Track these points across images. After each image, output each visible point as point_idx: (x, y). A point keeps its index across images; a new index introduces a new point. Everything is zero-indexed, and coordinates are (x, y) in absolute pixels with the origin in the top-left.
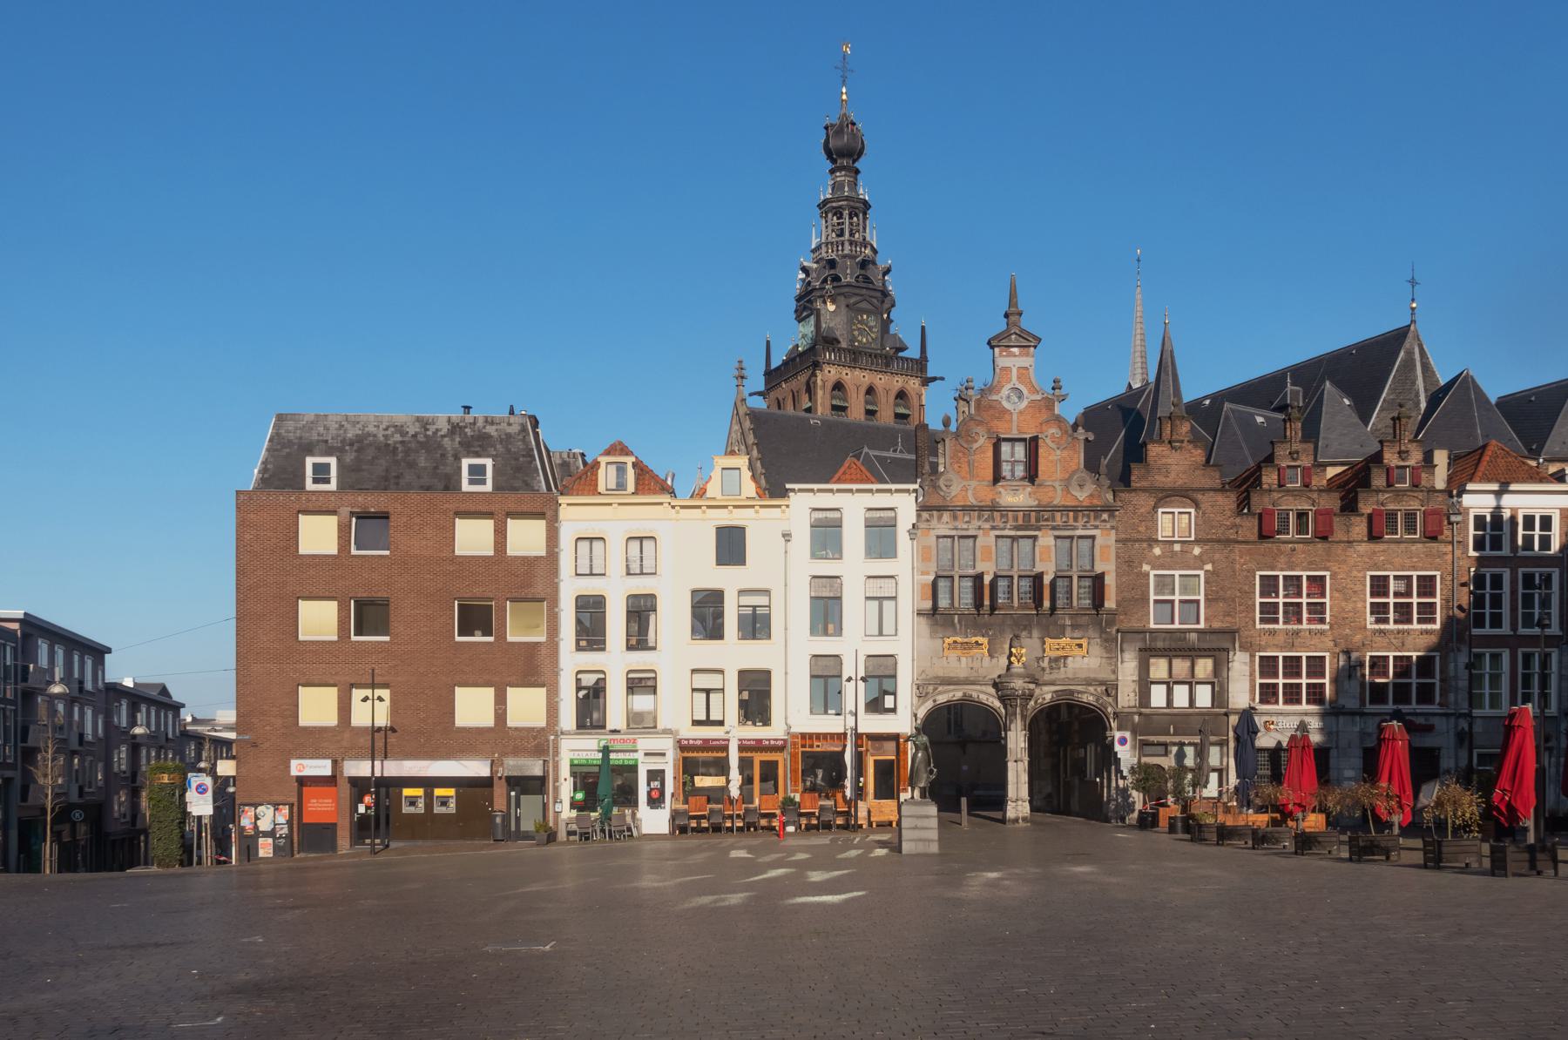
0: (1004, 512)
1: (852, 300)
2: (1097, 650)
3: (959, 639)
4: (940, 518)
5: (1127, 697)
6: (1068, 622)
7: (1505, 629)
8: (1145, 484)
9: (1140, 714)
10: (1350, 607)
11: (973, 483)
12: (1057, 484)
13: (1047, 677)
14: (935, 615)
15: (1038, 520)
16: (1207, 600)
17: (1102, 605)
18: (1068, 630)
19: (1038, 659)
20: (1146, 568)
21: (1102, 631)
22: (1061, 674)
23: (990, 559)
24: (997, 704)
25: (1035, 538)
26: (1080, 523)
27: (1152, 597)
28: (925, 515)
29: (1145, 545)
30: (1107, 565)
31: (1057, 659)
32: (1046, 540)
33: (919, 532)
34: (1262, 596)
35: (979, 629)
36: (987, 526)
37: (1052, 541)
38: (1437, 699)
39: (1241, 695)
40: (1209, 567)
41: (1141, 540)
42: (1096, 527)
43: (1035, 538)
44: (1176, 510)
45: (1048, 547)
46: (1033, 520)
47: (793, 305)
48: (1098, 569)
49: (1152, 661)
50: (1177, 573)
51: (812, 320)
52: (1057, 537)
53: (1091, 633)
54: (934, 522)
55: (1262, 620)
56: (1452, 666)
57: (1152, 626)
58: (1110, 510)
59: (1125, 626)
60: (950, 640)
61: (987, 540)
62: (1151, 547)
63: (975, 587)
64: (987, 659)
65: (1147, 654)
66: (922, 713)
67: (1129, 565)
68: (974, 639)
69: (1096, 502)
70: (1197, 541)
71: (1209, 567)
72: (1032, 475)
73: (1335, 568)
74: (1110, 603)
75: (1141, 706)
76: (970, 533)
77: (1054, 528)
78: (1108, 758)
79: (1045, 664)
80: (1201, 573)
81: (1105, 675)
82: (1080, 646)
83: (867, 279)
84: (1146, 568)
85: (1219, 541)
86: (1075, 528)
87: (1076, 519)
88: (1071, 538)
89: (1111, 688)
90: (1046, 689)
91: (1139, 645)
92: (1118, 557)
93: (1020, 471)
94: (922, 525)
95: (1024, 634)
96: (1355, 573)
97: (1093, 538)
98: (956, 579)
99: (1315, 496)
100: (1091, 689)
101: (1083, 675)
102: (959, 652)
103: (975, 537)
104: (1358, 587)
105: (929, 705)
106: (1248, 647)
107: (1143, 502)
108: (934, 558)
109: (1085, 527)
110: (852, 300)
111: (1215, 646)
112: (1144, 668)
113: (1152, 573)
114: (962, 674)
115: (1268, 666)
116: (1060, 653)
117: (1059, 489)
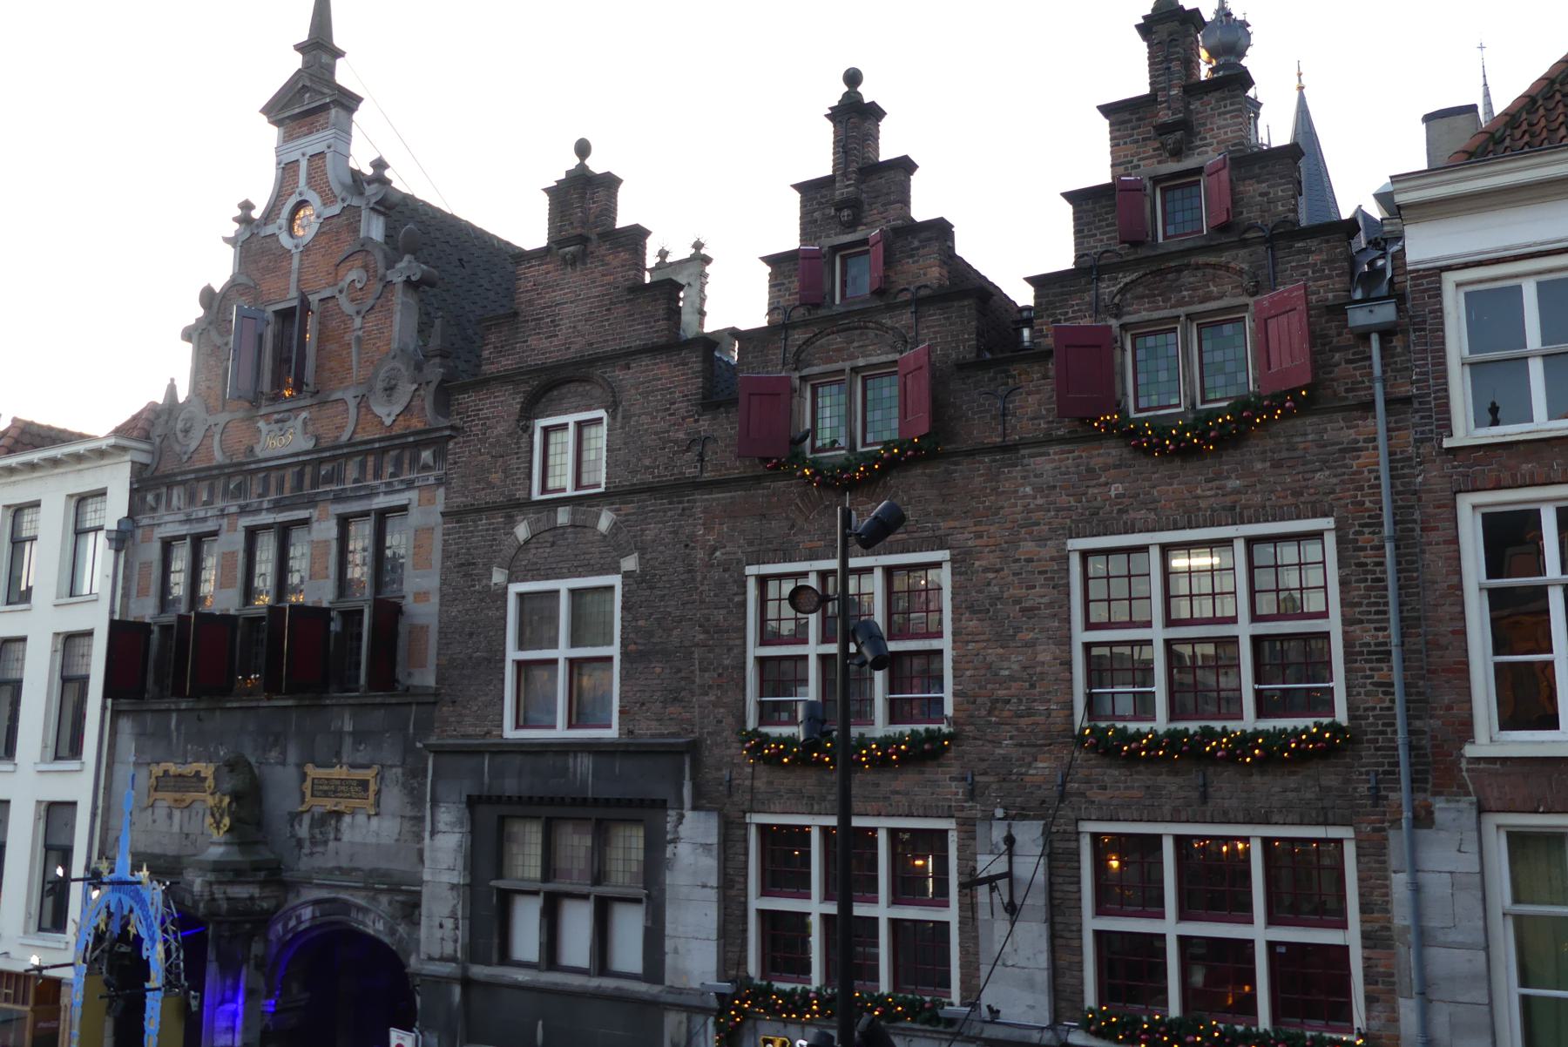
2: (394, 798)
3: (173, 769)
6: (348, 727)
8: (507, 363)
9: (467, 983)
10: (1014, 663)
22: (330, 857)
40: (630, 563)
42: (410, 485)
50: (563, 586)
56: (1399, 883)
57: (510, 732)
58: (438, 443)
60: (158, 770)
62: (511, 521)
67: (464, 571)
71: (630, 563)
73: (966, 538)
75: (474, 953)
76: (210, 526)
77: (339, 498)
79: (303, 831)
80: (615, 580)
84: (498, 577)
85: (651, 490)
86: (372, 494)
91: (468, 787)
92: (446, 556)
96: (1028, 547)
99: (905, 318)
104: (1040, 595)
107: (501, 405)
115: (784, 859)
116: (329, 804)
117: (352, 404)
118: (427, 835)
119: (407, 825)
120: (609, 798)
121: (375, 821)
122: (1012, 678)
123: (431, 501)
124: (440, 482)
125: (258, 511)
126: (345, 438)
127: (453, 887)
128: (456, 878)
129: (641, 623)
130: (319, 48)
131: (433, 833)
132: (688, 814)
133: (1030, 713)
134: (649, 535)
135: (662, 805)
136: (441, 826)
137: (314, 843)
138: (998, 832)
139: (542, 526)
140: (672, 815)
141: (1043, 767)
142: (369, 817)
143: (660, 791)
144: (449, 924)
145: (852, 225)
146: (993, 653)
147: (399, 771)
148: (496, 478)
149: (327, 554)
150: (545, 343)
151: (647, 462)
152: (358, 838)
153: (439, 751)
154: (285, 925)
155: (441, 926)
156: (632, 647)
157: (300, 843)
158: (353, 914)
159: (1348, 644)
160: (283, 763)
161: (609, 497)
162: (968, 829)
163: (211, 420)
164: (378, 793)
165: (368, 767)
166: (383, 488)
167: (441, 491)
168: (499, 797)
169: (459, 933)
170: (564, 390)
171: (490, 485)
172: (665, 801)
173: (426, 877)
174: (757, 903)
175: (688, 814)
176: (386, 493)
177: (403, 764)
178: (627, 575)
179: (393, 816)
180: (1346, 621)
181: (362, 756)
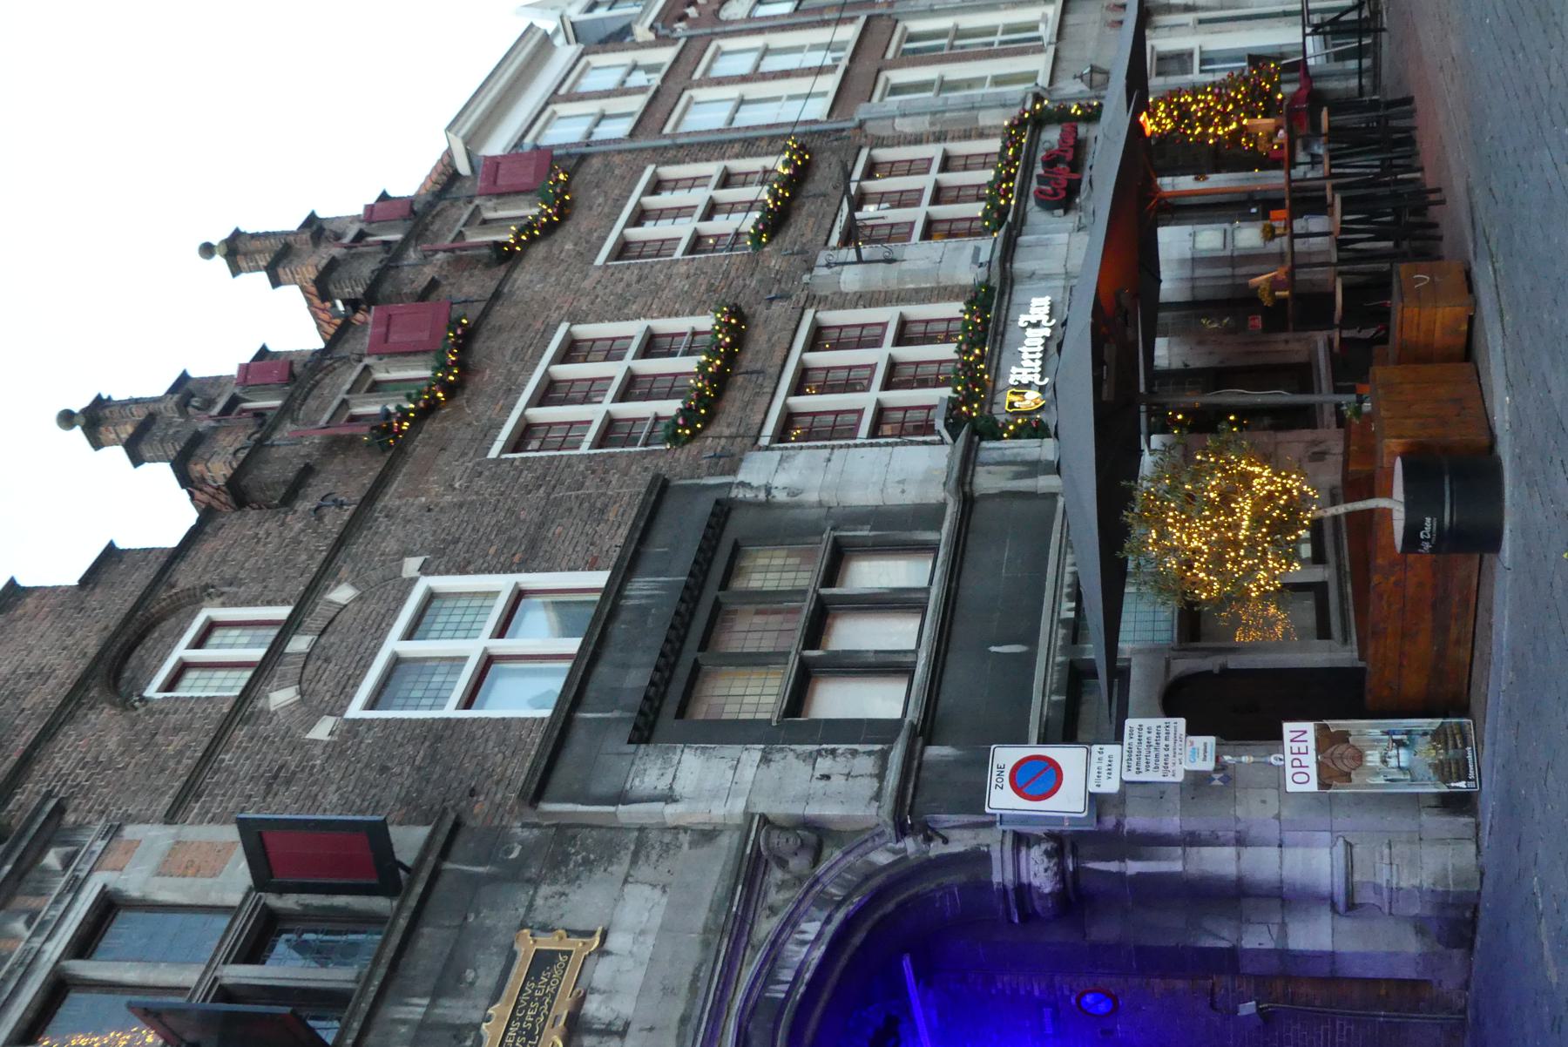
2: (586, 901)
16: (524, 566)
18: (454, 1010)
20: (322, 731)
21: (515, 874)
27: (450, 711)
29: (241, 734)
42: (76, 886)
44: (182, 651)
50: (394, 643)
81: (710, 873)
84: (322, 731)
91: (616, 742)
96: (587, 284)
97: (109, 907)
100: (766, 927)
113: (355, 710)
118: (671, 812)
119: (644, 871)
122: (693, 285)
123: (134, 844)
124: (113, 832)
127: (766, 759)
128: (754, 753)
129: (492, 551)
132: (741, 477)
133: (726, 274)
135: (724, 510)
136: (663, 785)
139: (292, 670)
142: (602, 952)
143: (704, 506)
144: (824, 764)
145: (210, 403)
146: (667, 294)
147: (545, 890)
148: (178, 741)
150: (46, 689)
151: (304, 557)
152: (635, 977)
153: (538, 790)
155: (827, 777)
156: (516, 559)
158: (779, 992)
159: (737, 156)
162: (813, 300)
164: (571, 932)
165: (511, 957)
166: (37, 942)
167: (130, 831)
168: (646, 698)
169: (842, 748)
170: (133, 661)
171: (180, 753)
172: (718, 502)
175: (741, 477)
176: (49, 938)
177: (535, 883)
178: (425, 570)
179: (618, 900)
180: (722, 157)
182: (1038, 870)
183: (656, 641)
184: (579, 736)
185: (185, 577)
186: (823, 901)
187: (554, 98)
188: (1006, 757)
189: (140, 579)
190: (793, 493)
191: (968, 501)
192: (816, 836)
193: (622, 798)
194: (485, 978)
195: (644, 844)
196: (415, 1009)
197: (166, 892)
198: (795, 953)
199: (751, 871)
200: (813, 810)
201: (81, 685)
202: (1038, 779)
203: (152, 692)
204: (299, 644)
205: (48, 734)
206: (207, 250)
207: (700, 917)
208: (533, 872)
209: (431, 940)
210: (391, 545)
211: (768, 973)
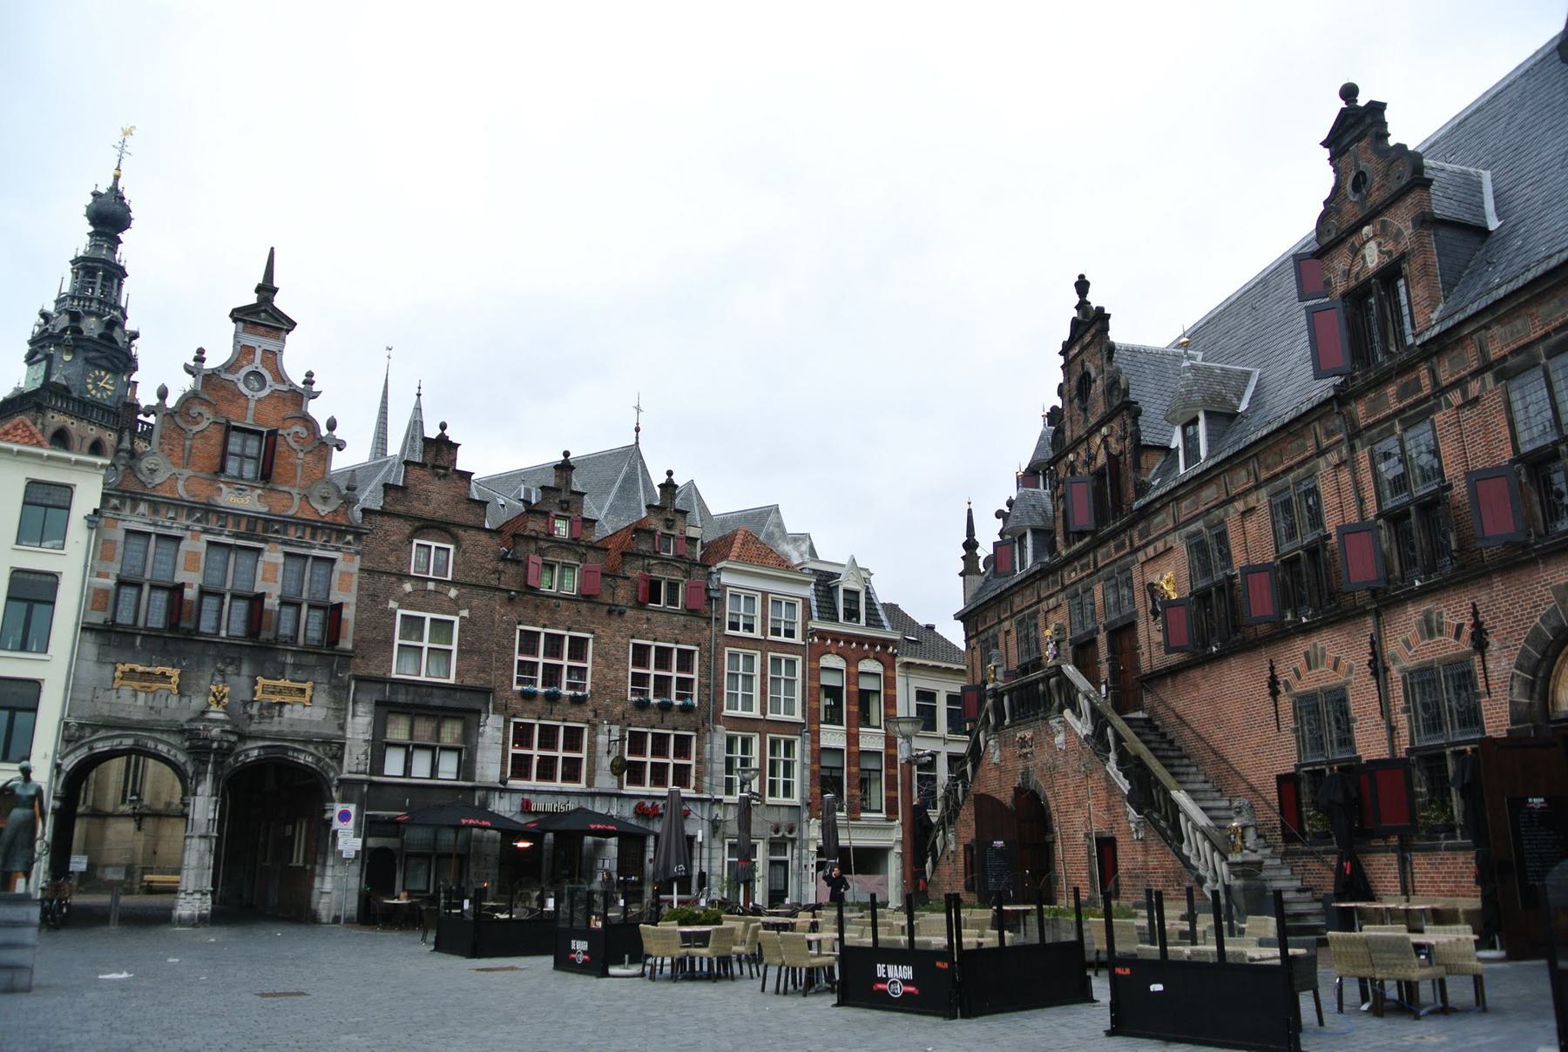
0: (224, 514)
1: (92, 354)
2: (322, 698)
3: (140, 669)
4: (134, 509)
5: (354, 762)
7: (756, 713)
10: (611, 675)
11: (188, 473)
12: (295, 492)
13: (254, 728)
14: (107, 634)
15: (265, 530)
16: (460, 650)
17: (337, 643)
18: (288, 673)
19: (245, 704)
20: (392, 604)
21: (333, 675)
22: (273, 726)
23: (196, 569)
24: (181, 758)
25: (259, 551)
26: (319, 541)
27: (397, 641)
28: (115, 502)
30: (345, 595)
31: (271, 706)
32: (273, 555)
33: (103, 521)
34: (521, 652)
35: (169, 657)
36: (198, 527)
37: (281, 559)
38: (693, 782)
39: (489, 768)
40: (465, 613)
41: (390, 574)
42: (338, 549)
43: (259, 551)
44: (434, 544)
45: (275, 565)
46: (260, 528)
47: (26, 348)
48: (335, 598)
49: (391, 717)
50: (428, 616)
51: (44, 364)
52: (287, 554)
53: (320, 676)
54: (127, 511)
55: (520, 681)
57: (394, 675)
58: (358, 536)
59: (362, 672)
60: (127, 667)
61: (195, 544)
63: (170, 602)
64: (173, 701)
65: (385, 710)
66: (69, 764)
67: (371, 599)
68: (159, 670)
69: (339, 519)
70: (453, 583)
71: (465, 613)
72: (266, 475)
74: (346, 644)
76: (174, 532)
77: (285, 543)
78: (323, 836)
79: (254, 711)
81: (330, 730)
82: (303, 691)
83: (114, 341)
84: (392, 604)
86: (312, 547)
87: (313, 537)
88: (306, 557)
89: (335, 747)
90: (250, 744)
91: (376, 697)
92: (360, 588)
93: (249, 470)
94: (108, 514)
95: (230, 669)
97: (333, 561)
98: (146, 588)
100: (311, 749)
101: (302, 729)
102: (136, 685)
103: (178, 539)
104: (621, 655)
105: (82, 753)
106: (504, 710)
108: (118, 557)
109: (323, 547)
110: (92, 354)
111: (464, 705)
112: (379, 727)
113: (400, 612)
114: (138, 716)
115: (522, 735)
116: (277, 698)
117: (297, 498)
120: (455, 708)
121: (308, 710)
124: (358, 553)
125: (220, 534)
126: (290, 513)
128: (368, 737)
130: (267, 289)
131: (354, 715)
134: (475, 603)
135: (478, 712)
137: (261, 716)
138: (606, 728)
140: (483, 716)
141: (619, 709)
143: (478, 706)
148: (392, 559)
149: (276, 570)
152: (296, 716)
153: (359, 679)
154: (236, 760)
157: (251, 717)
160: (238, 675)
161: (453, 583)
162: (594, 727)
163: (175, 470)
173: (349, 735)
174: (511, 751)
181: (300, 675)
182: (328, 816)
183: (417, 700)
184: (380, 686)
185: (468, 537)
186: (319, 760)
187: (765, 594)
188: (352, 808)
189: (471, 519)
190: (482, 735)
191: (474, 789)
192: (340, 759)
193: (355, 702)
194: (297, 677)
195: (340, 713)
196: (290, 660)
197: (335, 577)
198: (302, 757)
199: (326, 741)
200: (346, 756)
201: (419, 519)
202: (345, 816)
203: (416, 541)
204: (431, 586)
205: (398, 516)
206: (670, 473)
207: (314, 730)
208: (334, 681)
209: (311, 659)
210: (475, 603)
211: (295, 750)
